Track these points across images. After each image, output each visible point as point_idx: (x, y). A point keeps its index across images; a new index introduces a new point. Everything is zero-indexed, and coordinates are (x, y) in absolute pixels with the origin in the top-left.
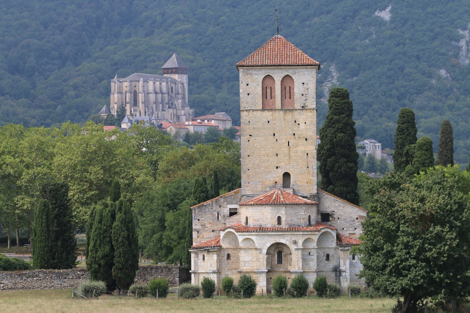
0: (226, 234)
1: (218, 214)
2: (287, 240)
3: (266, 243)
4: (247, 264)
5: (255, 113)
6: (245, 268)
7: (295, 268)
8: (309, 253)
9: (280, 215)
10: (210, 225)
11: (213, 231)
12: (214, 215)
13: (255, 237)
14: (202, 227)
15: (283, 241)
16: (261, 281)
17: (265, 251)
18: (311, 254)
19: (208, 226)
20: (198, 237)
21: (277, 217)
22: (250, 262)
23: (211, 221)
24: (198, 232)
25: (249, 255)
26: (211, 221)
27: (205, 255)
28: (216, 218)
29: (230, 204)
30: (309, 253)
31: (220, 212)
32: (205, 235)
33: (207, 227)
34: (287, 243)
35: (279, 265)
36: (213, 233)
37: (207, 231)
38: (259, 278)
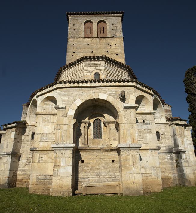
2: (110, 95)
3: (75, 100)
4: (45, 138)
5: (78, 39)
6: (41, 144)
7: (126, 141)
8: (144, 121)
9: (98, 71)
13: (58, 91)
15: (103, 96)
16: (62, 165)
17: (72, 112)
18: (146, 122)
21: (93, 74)
22: (50, 135)
25: (50, 124)
30: (144, 121)
34: (111, 100)
35: (97, 140)
38: (58, 159)
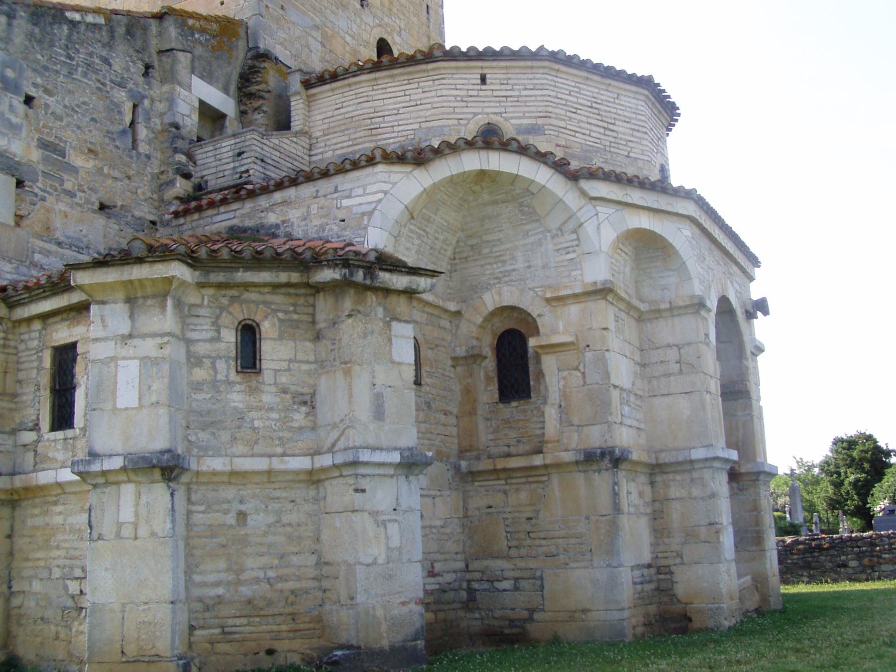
0: (430, 195)
1: (135, 106)
10: (90, 164)
11: (103, 207)
12: (115, 108)
14: (45, 160)
19: (78, 160)
20: (19, 218)
23: (95, 136)
24: (20, 184)
26: (95, 136)
27: (268, 328)
28: (124, 132)
29: (202, 77)
31: (146, 102)
32: (58, 223)
33: (74, 170)
36: (100, 221)
37: (71, 194)
